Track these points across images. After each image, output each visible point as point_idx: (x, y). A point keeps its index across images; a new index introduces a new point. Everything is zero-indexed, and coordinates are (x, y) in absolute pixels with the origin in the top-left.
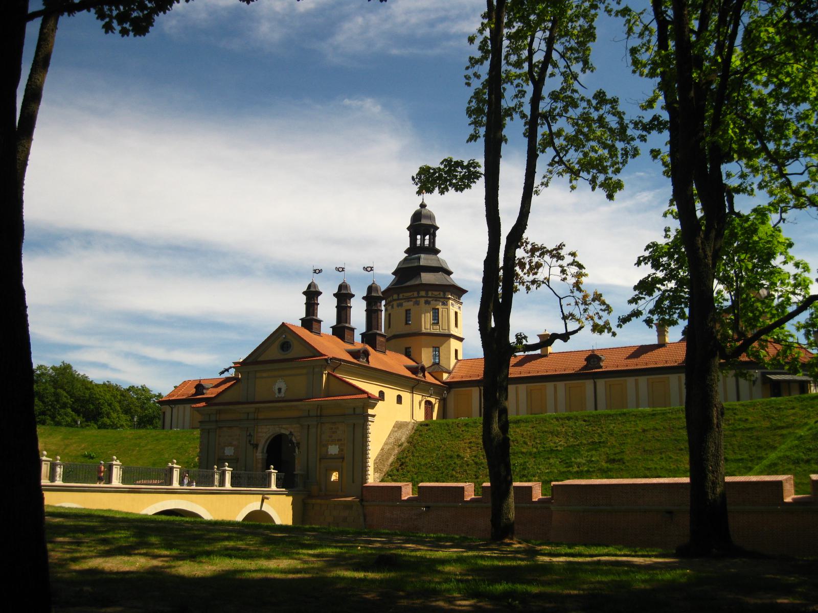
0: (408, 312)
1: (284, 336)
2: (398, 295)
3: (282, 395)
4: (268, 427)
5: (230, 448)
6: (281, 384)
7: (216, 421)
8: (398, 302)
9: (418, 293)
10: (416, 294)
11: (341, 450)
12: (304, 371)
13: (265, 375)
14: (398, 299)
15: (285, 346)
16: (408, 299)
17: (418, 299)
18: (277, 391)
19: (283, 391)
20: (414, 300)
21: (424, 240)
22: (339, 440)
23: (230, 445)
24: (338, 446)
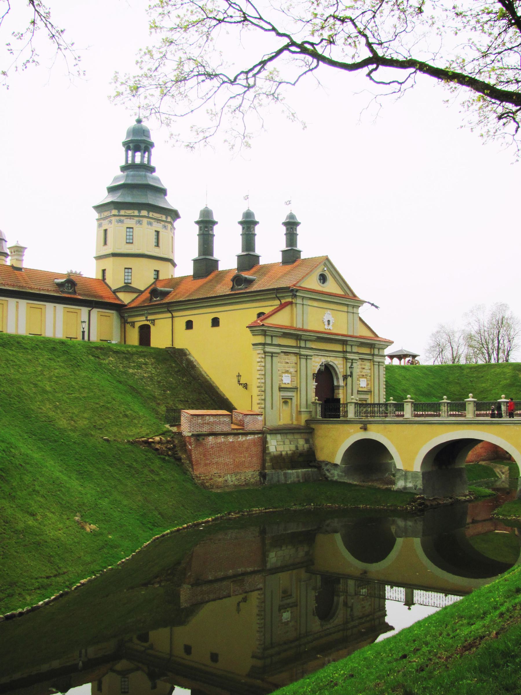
0: (158, 232)
1: (325, 269)
2: (148, 213)
3: (330, 327)
4: (319, 357)
5: (286, 375)
6: (328, 316)
7: (279, 345)
8: (149, 220)
9: (167, 218)
10: (164, 218)
11: (368, 385)
12: (345, 308)
13: (315, 304)
14: (148, 217)
15: (323, 278)
16: (158, 220)
17: (166, 224)
18: (326, 323)
19: (331, 324)
20: (163, 223)
21: (144, 157)
22: (366, 375)
23: (287, 372)
24: (365, 380)
